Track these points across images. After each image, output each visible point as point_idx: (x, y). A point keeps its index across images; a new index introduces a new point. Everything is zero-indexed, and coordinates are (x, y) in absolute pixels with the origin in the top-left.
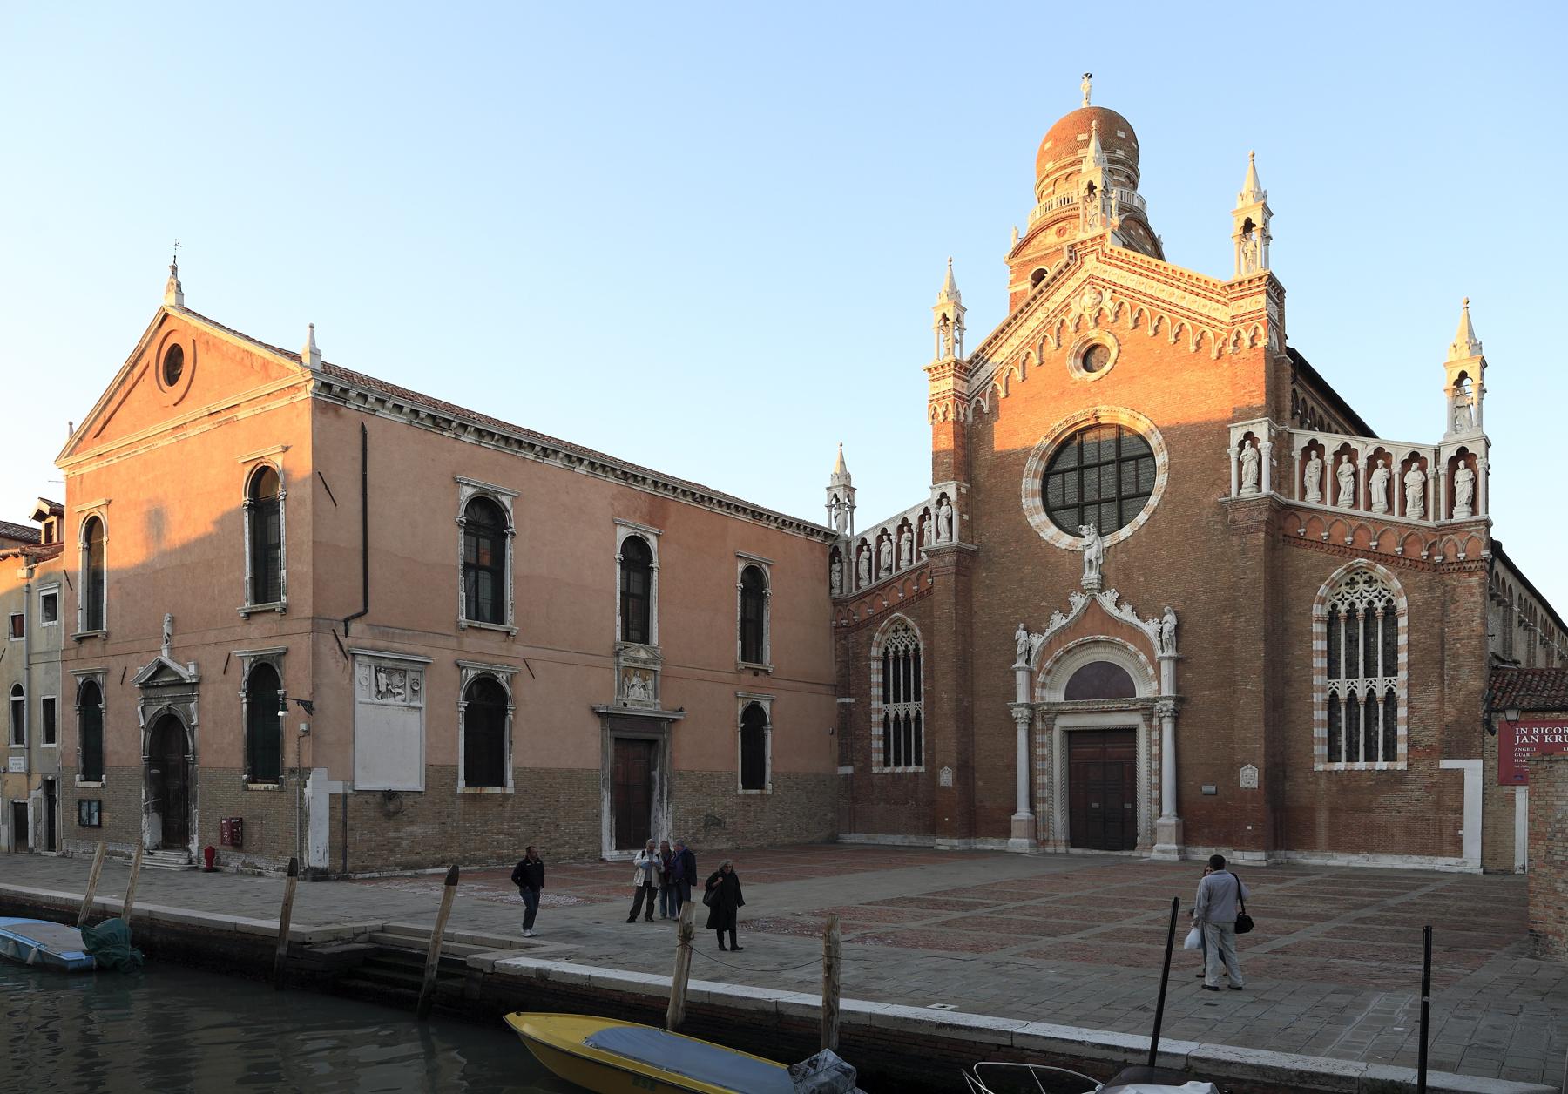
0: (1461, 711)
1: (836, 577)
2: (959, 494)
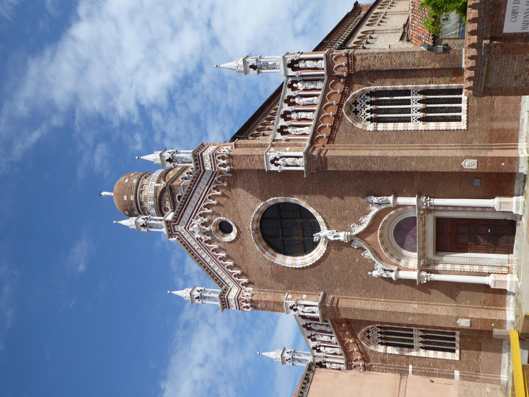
0: (433, 61)
2: (291, 299)
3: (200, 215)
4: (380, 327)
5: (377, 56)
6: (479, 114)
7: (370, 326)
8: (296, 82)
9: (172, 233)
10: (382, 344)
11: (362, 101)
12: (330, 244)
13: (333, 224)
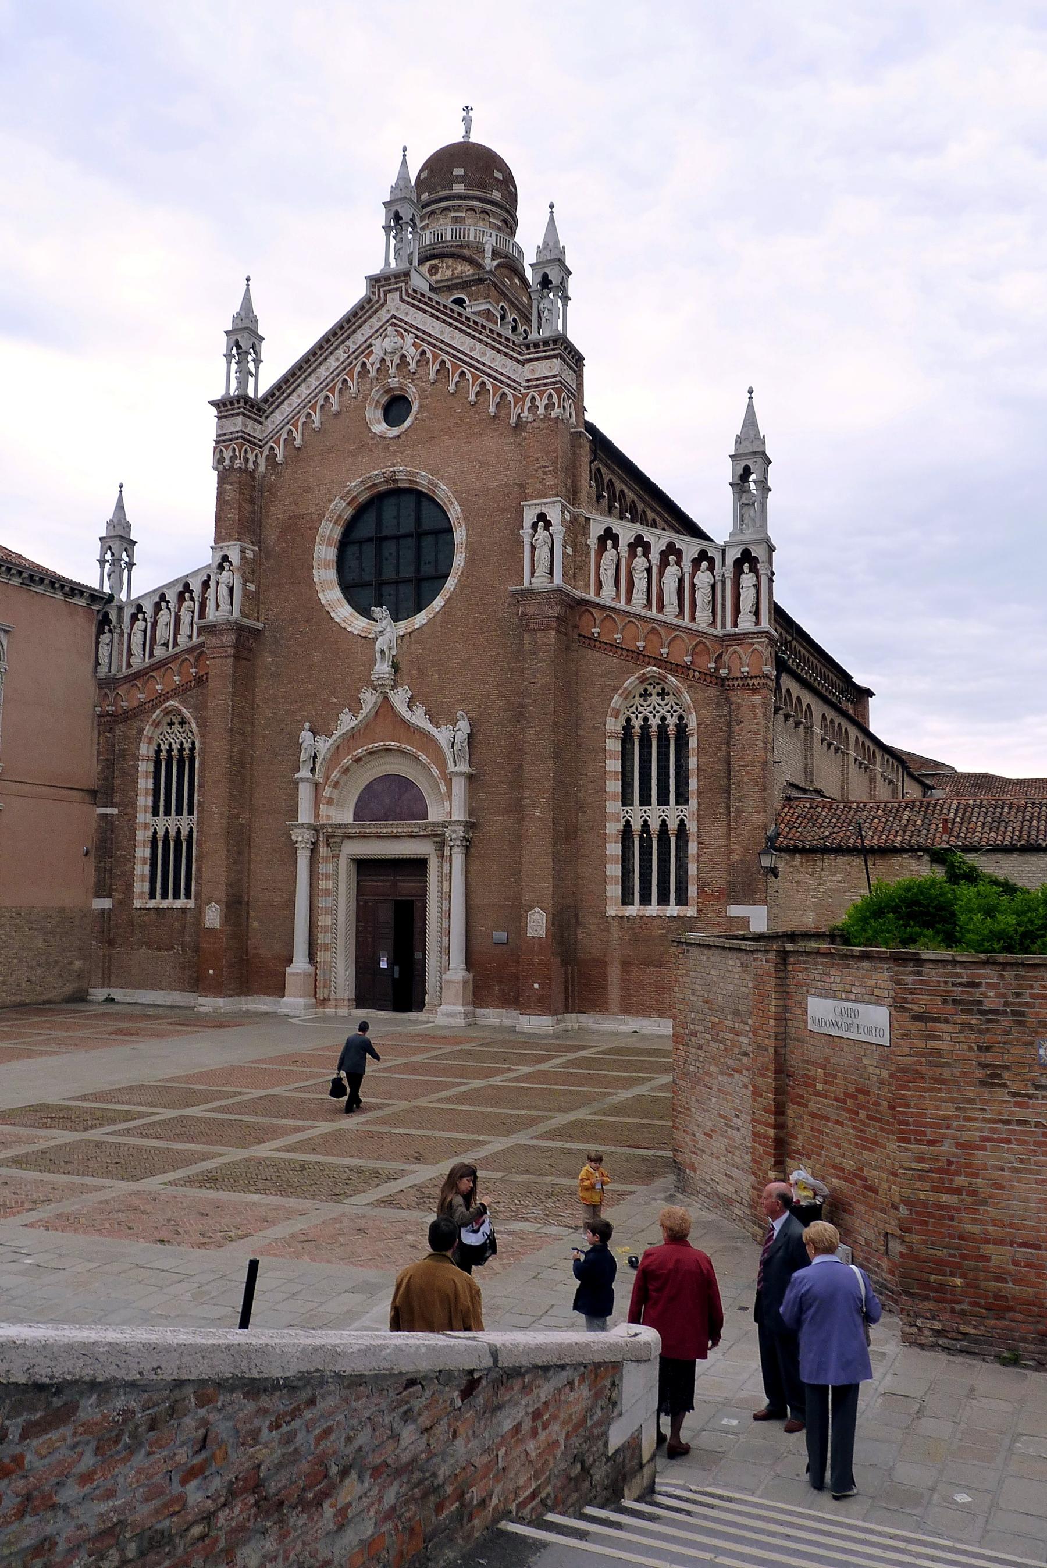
0: (746, 849)
1: (104, 651)
2: (243, 558)
3: (423, 353)
4: (192, 749)
5: (760, 737)
6: (636, 939)
7: (194, 726)
8: (711, 568)
9: (383, 286)
10: (158, 751)
11: (668, 708)
12: (368, 641)
13: (409, 647)
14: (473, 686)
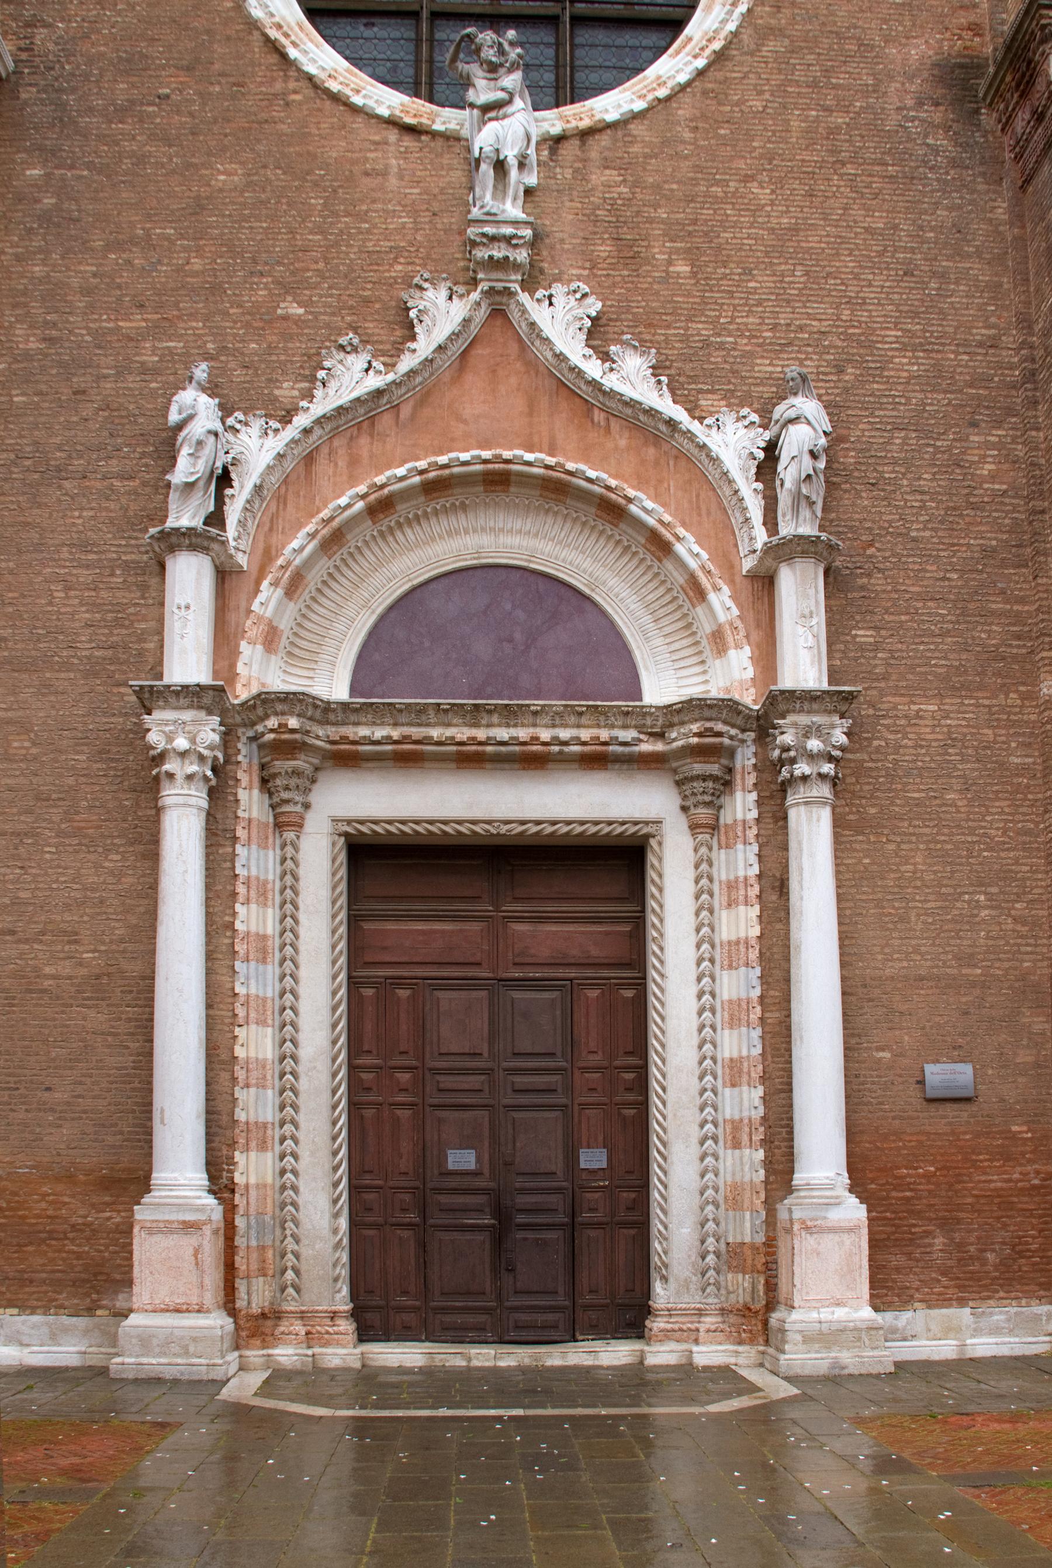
14: (814, 308)
